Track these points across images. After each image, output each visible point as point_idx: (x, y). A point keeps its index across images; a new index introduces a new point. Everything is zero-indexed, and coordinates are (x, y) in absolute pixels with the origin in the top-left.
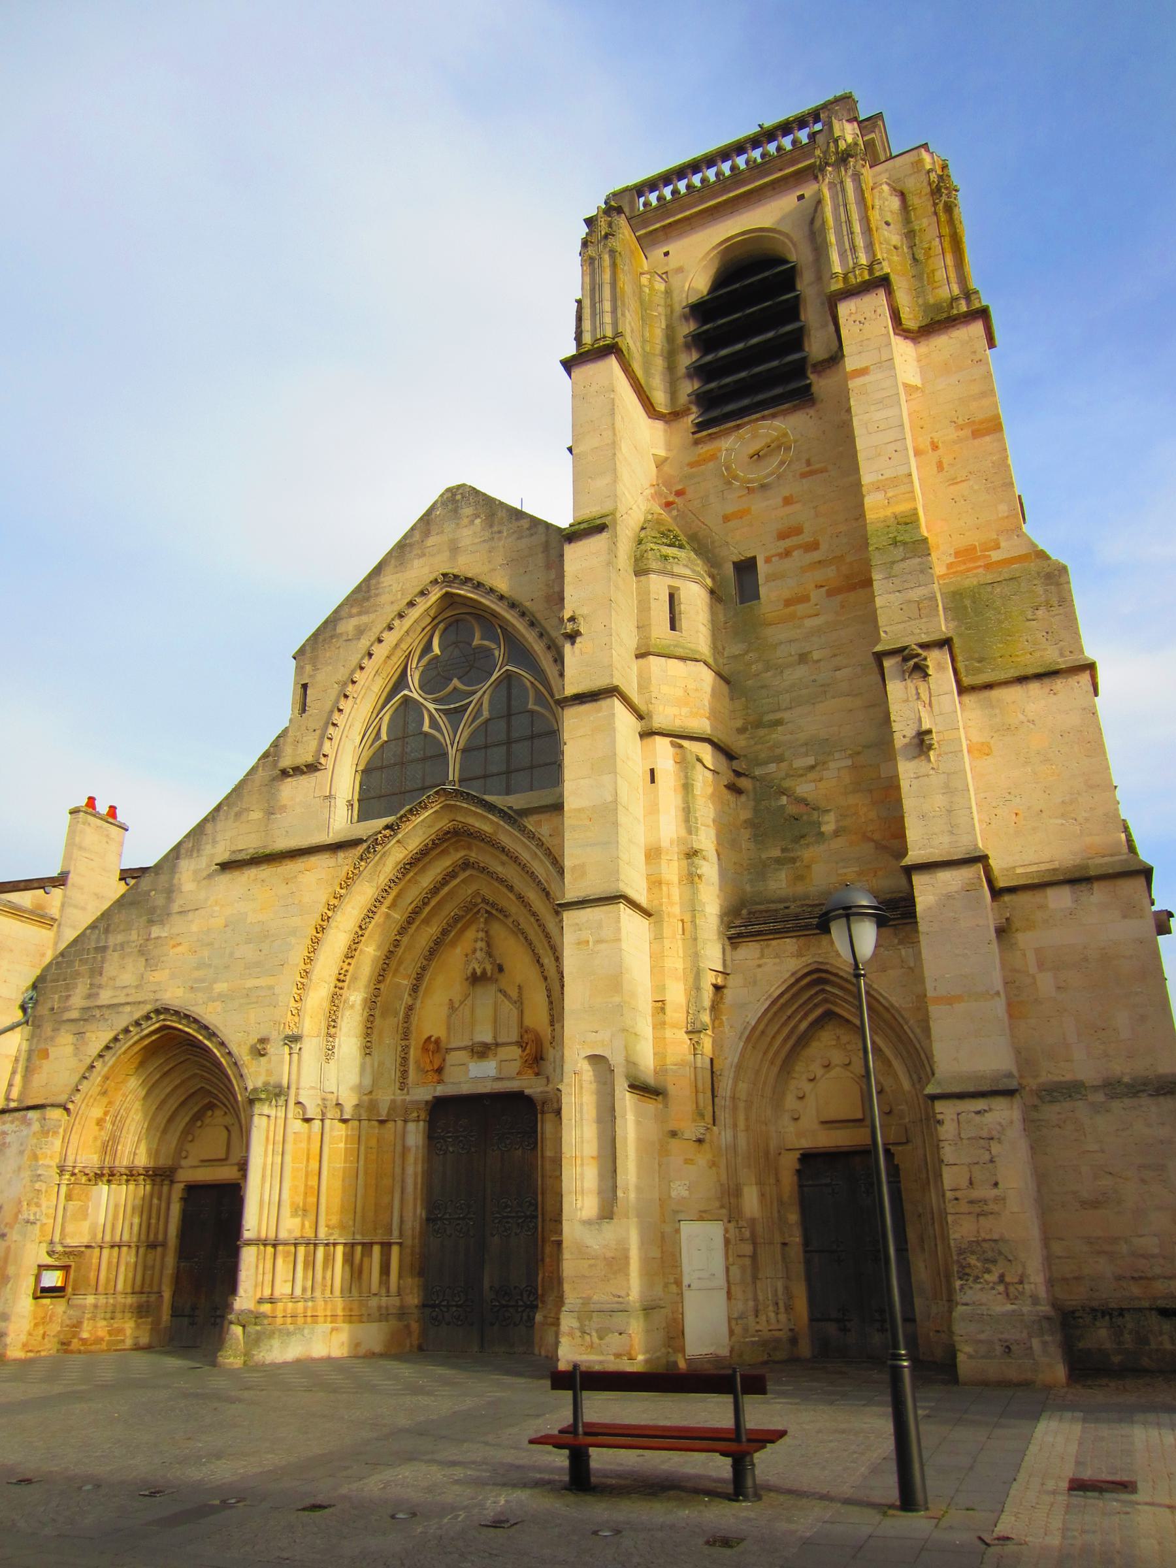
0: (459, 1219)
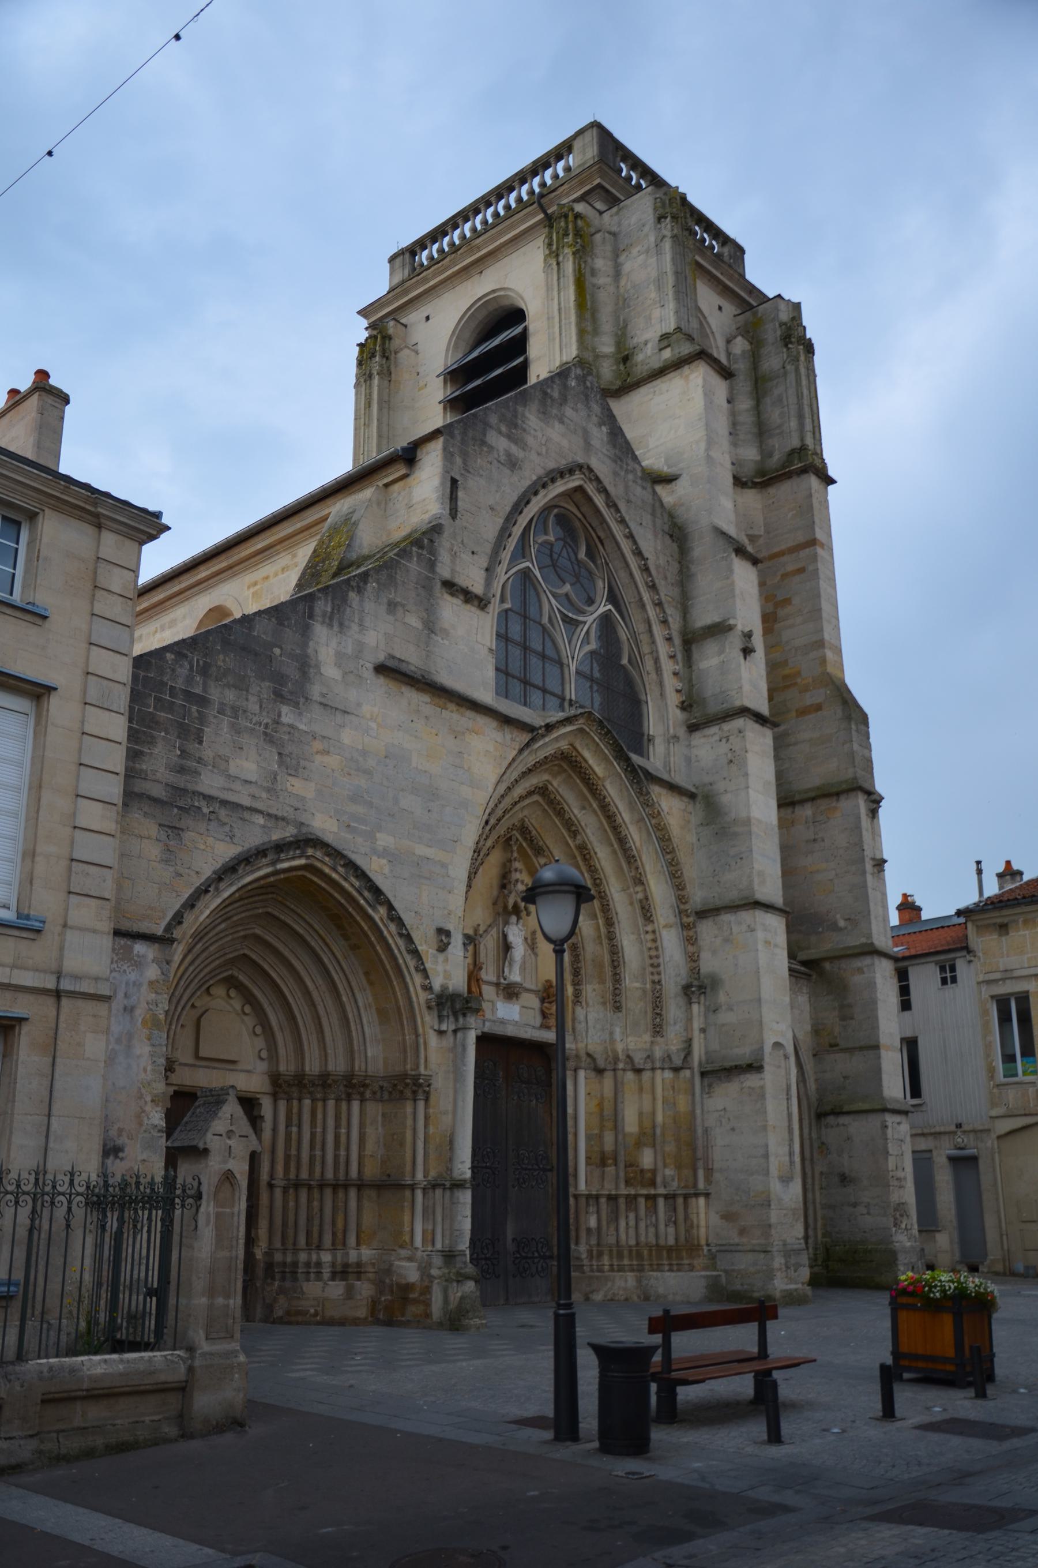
0: (486, 1167)
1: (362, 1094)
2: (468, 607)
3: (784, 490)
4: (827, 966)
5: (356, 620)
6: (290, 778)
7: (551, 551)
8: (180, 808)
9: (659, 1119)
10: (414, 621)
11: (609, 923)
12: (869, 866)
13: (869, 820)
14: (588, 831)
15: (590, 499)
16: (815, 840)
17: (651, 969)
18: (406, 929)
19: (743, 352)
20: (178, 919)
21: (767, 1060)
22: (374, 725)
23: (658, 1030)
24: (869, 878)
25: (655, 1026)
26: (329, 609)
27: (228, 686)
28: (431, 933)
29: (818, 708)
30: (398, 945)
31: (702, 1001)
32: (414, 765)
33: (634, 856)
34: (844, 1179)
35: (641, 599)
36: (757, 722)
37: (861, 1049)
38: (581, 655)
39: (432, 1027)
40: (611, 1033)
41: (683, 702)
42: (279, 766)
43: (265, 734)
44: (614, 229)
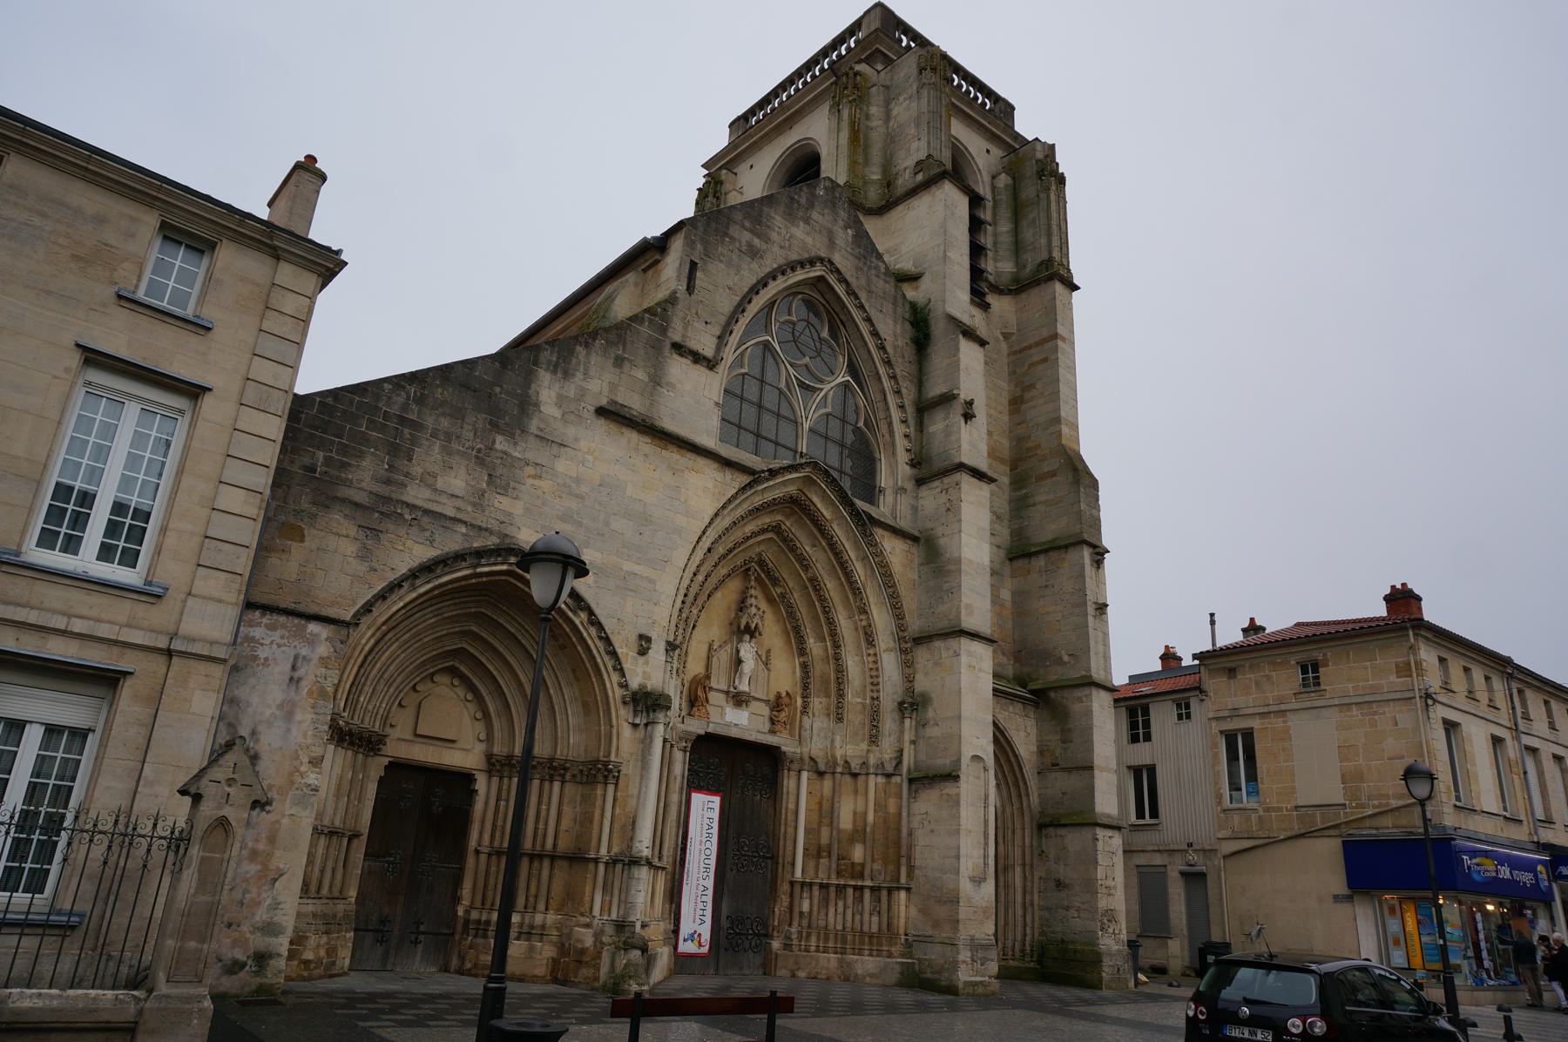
1: (563, 776)
2: (698, 367)
3: (1035, 297)
4: (1052, 695)
5: (581, 370)
6: (497, 496)
7: (794, 329)
8: (382, 513)
9: (871, 818)
10: (640, 374)
11: (836, 646)
12: (1091, 610)
13: (1094, 570)
14: (818, 565)
15: (832, 289)
16: (1046, 586)
17: (871, 687)
18: (605, 633)
19: (1006, 186)
20: (367, 608)
21: (963, 766)
22: (590, 458)
23: (874, 740)
24: (1090, 619)
25: (871, 736)
26: (554, 359)
27: (444, 415)
28: (633, 638)
29: (1053, 474)
30: (597, 647)
31: (914, 717)
32: (628, 493)
33: (859, 589)
34: (1060, 885)
35: (878, 373)
36: (973, 476)
37: (1078, 768)
38: (816, 415)
39: (627, 720)
40: (833, 741)
41: (912, 460)
42: (488, 485)
43: (477, 457)
44: (888, 83)
